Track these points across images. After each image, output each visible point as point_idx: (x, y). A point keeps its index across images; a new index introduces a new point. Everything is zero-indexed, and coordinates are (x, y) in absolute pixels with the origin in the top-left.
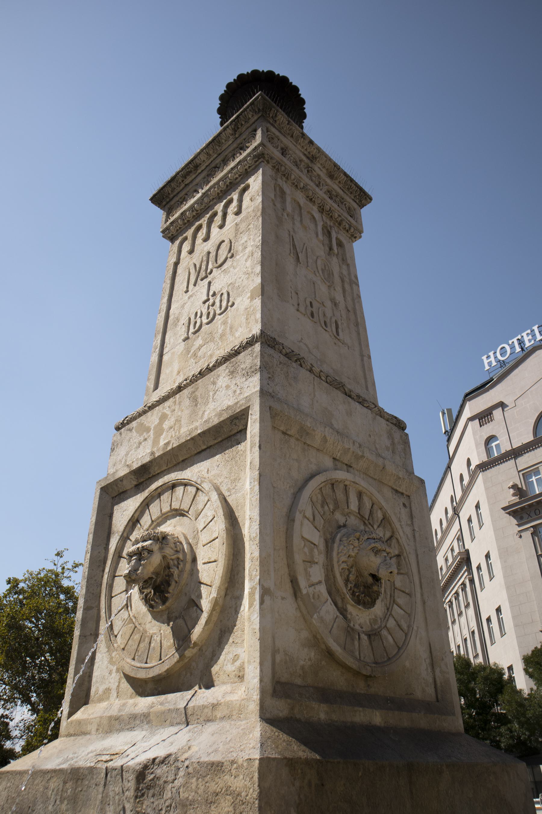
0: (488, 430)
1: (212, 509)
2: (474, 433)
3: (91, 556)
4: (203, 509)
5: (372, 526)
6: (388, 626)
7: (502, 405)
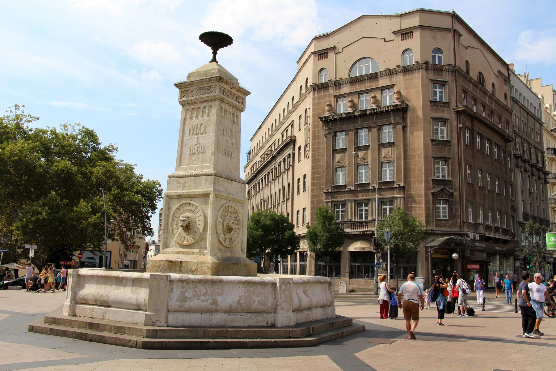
0: (323, 63)
1: (201, 213)
2: (315, 65)
7: (334, 48)
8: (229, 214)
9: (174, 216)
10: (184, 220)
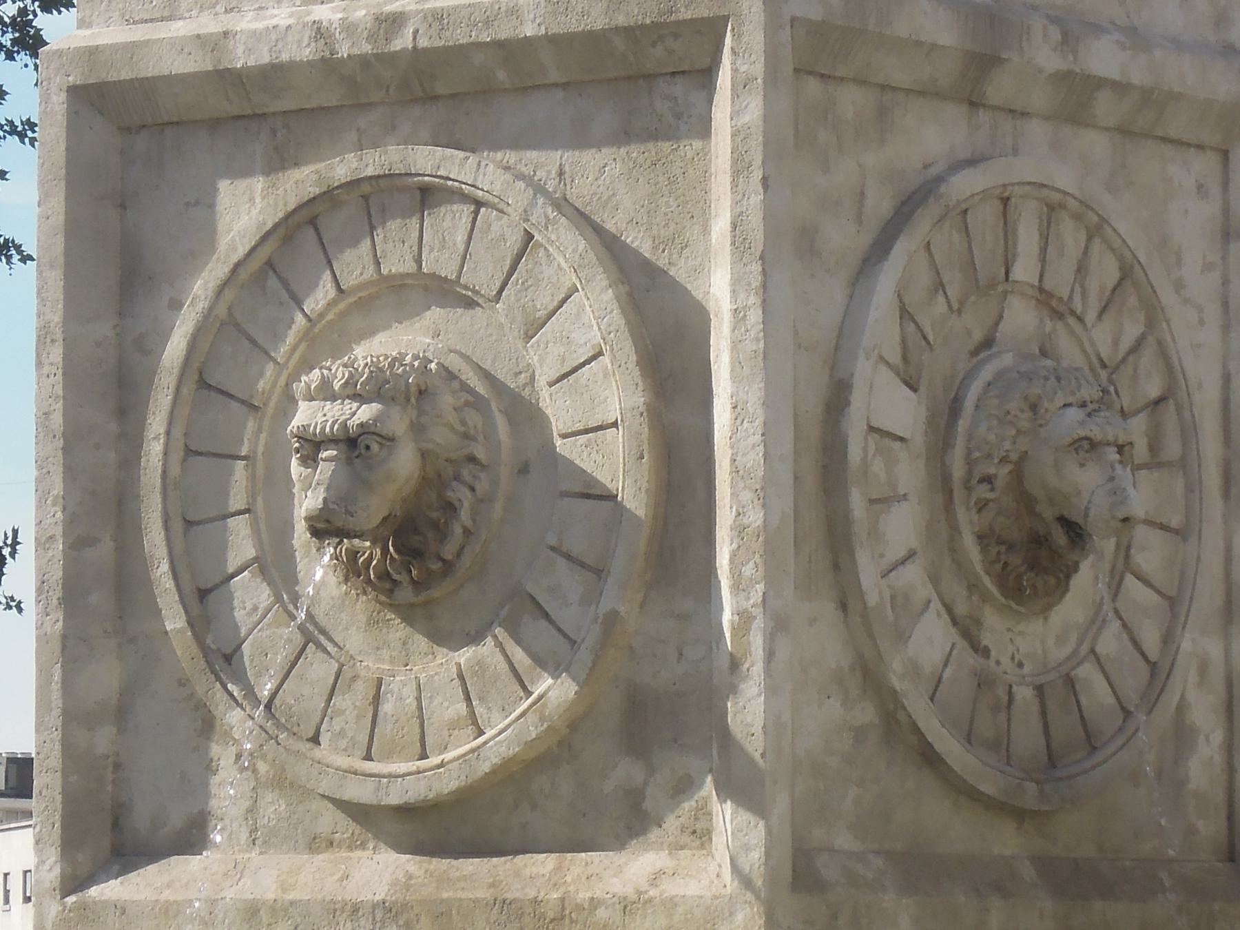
3: (66, 357)
4: (554, 312)
5: (1080, 319)
6: (1098, 649)
8: (1021, 317)
9: (202, 380)
10: (352, 443)
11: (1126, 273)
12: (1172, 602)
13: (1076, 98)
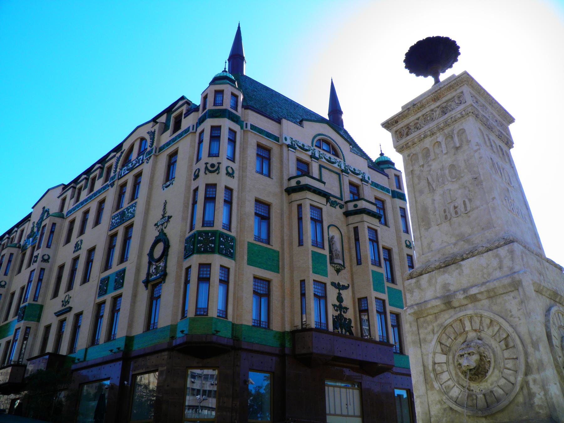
8: (472, 335)
11: (491, 321)
12: (516, 371)
13: (474, 299)
